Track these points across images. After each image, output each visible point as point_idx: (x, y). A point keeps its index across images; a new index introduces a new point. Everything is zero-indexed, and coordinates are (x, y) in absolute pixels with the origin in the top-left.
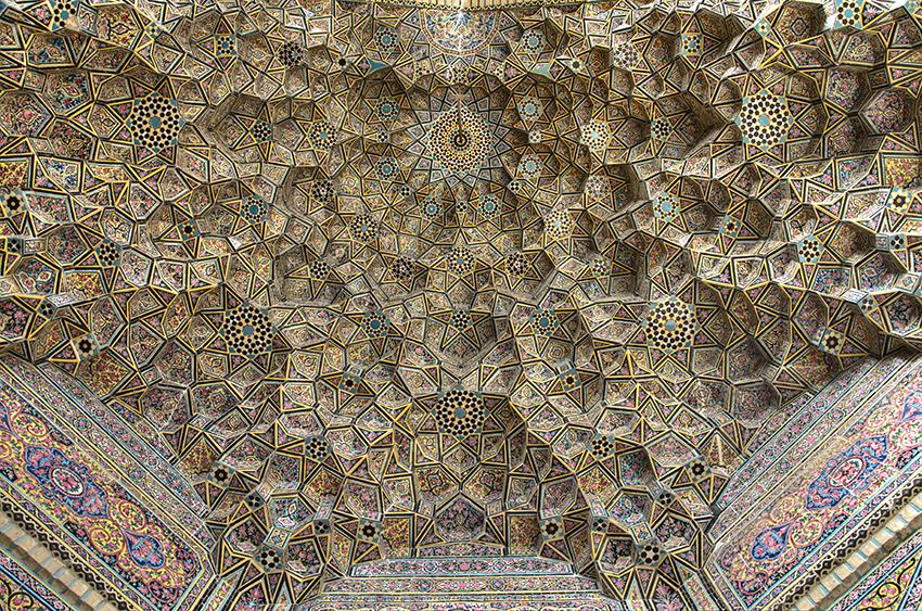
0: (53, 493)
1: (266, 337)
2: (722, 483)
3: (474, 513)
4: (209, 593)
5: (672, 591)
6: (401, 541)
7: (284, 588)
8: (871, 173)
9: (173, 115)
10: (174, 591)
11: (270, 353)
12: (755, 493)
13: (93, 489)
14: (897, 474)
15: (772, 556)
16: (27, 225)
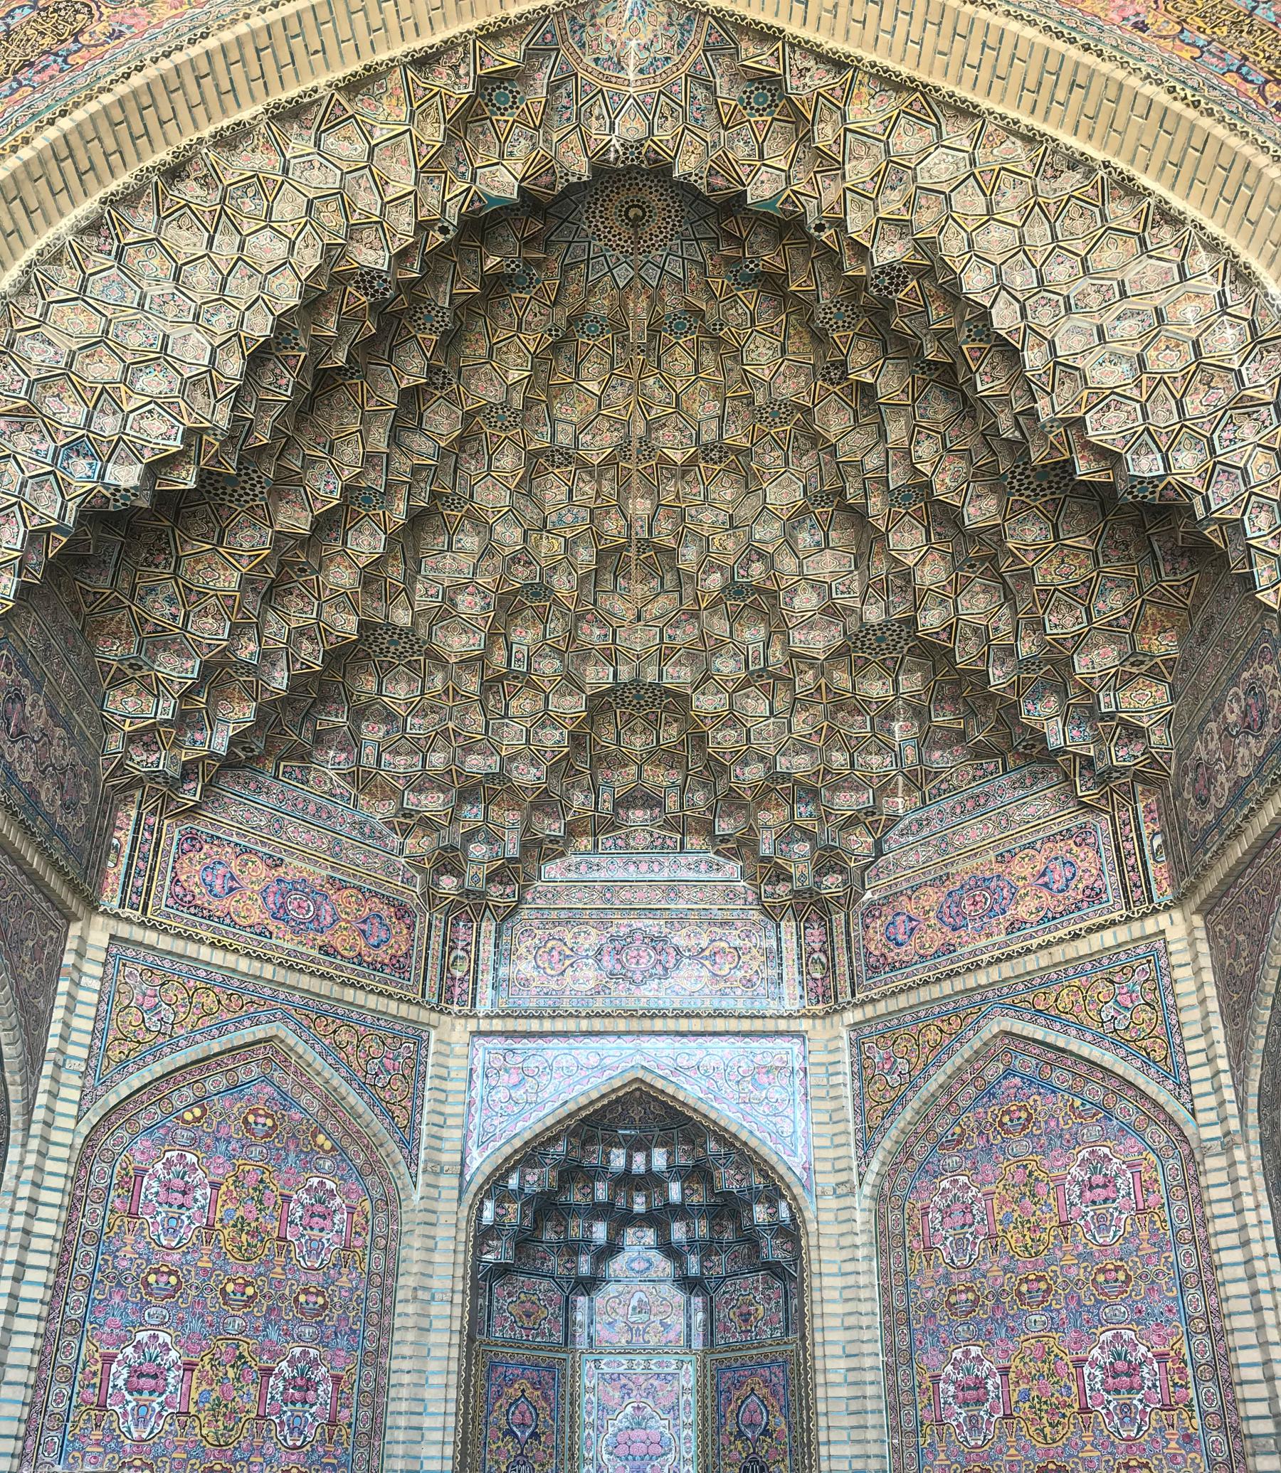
0: (298, 928)
1: (416, 647)
2: (893, 820)
3: (653, 798)
4: (429, 938)
5: (822, 919)
6: (585, 833)
7: (488, 912)
8: (1126, 615)
9: (254, 476)
10: (407, 955)
11: (422, 658)
12: (912, 858)
13: (319, 899)
14: (1002, 937)
15: (897, 944)
16: (161, 688)
